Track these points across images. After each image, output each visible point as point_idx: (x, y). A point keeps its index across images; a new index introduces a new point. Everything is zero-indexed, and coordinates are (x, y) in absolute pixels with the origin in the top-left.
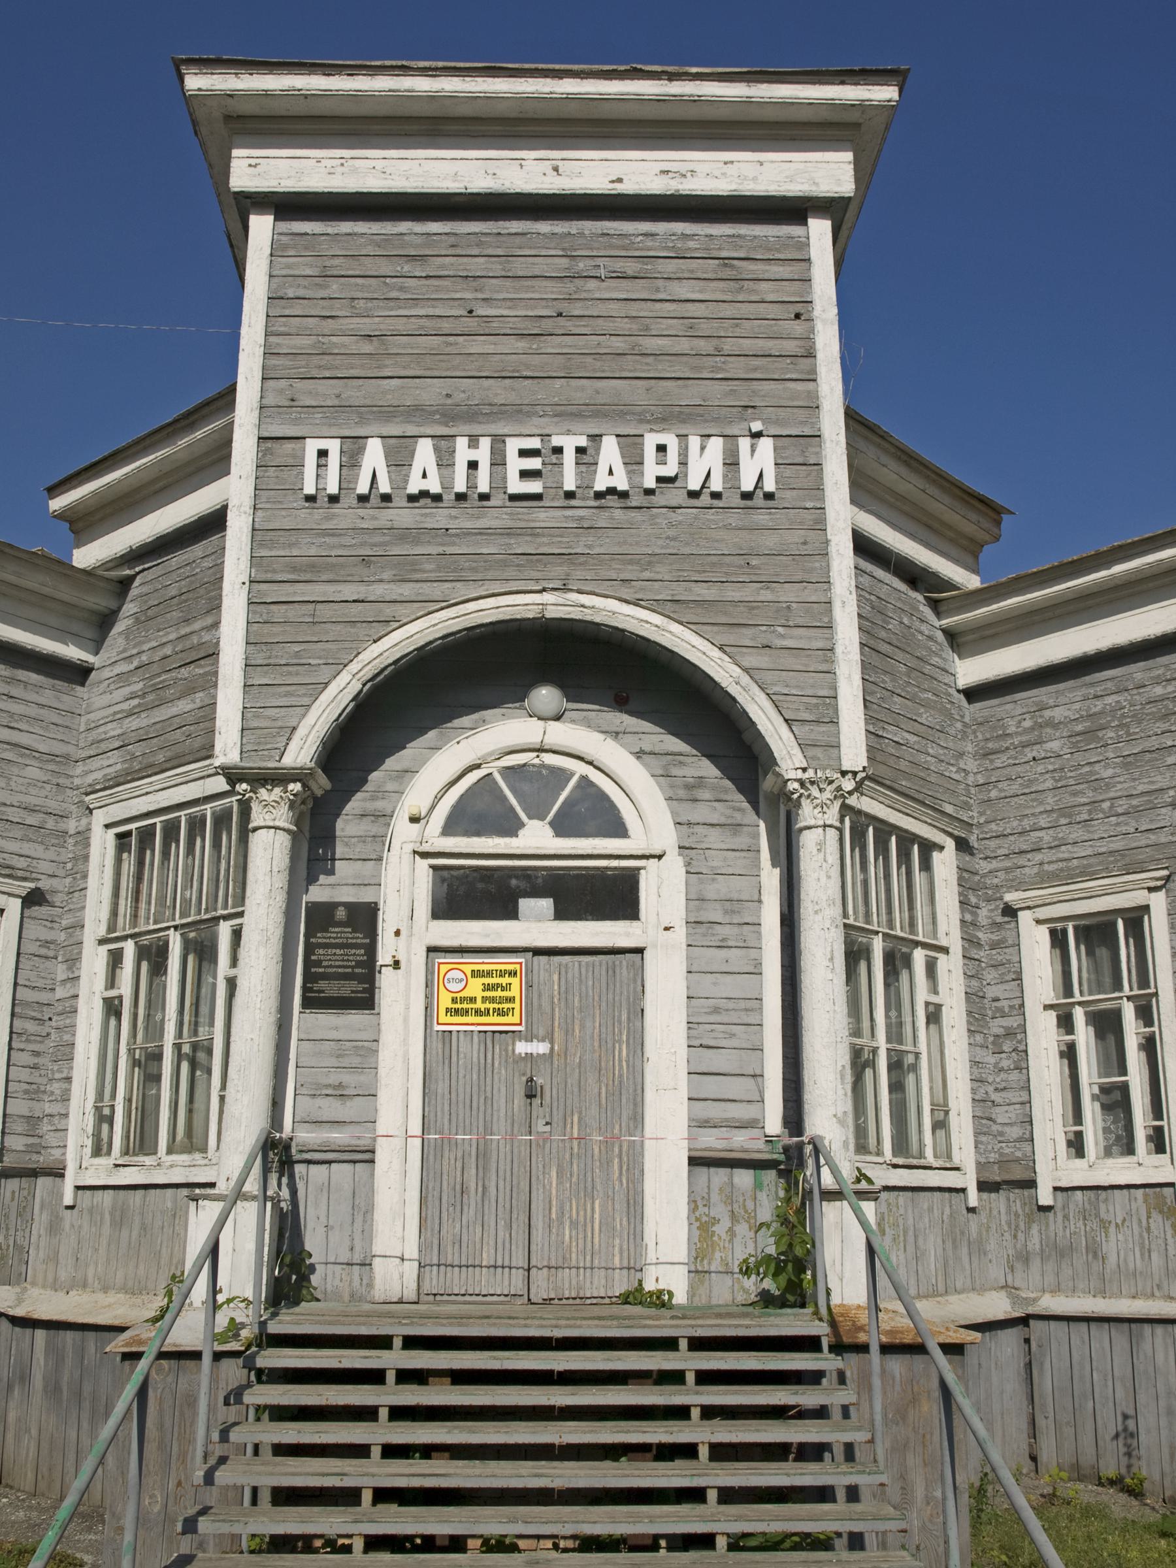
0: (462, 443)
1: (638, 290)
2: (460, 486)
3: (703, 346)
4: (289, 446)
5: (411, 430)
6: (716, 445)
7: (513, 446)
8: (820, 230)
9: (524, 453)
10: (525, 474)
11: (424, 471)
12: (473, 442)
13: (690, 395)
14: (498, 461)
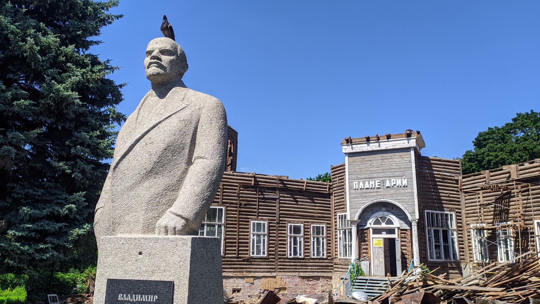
1: (390, 160)
3: (399, 167)
6: (400, 180)
7: (377, 181)
8: (412, 152)
11: (367, 186)
13: (397, 174)
14: (375, 184)
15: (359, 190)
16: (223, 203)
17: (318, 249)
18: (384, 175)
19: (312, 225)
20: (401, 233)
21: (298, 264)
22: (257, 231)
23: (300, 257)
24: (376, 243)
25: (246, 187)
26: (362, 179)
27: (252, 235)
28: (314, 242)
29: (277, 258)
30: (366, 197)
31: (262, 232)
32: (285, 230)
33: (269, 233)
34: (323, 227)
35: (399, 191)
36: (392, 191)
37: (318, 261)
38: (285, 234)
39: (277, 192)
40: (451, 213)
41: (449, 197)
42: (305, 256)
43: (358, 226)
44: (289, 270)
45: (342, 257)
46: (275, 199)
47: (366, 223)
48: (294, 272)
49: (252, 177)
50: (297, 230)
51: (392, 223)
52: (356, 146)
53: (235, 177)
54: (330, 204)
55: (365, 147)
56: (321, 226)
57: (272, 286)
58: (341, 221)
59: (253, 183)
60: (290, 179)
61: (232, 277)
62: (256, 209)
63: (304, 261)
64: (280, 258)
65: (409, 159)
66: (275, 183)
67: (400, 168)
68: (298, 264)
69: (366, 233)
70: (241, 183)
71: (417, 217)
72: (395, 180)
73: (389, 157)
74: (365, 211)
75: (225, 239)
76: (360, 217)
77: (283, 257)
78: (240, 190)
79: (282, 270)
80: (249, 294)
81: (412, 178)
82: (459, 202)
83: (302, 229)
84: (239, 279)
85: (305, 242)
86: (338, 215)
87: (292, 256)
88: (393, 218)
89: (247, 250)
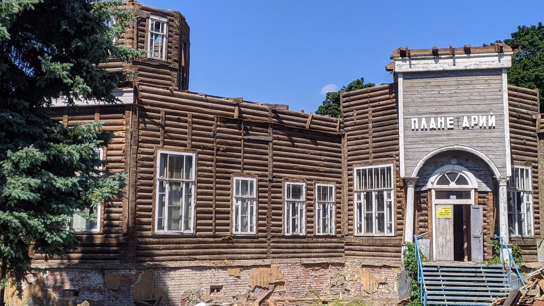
0: (439, 118)
2: (439, 127)
4: (408, 120)
5: (430, 116)
6: (485, 117)
7: (448, 119)
8: (505, 76)
9: (450, 120)
10: (451, 124)
11: (433, 125)
12: (441, 119)
13: (479, 108)
14: (446, 122)
15: (420, 131)
16: (193, 146)
17: (324, 220)
18: (459, 108)
19: (317, 185)
20: (479, 197)
21: (297, 245)
22: (242, 194)
23: (301, 234)
24: (442, 211)
25: (226, 120)
26: (424, 114)
27: (234, 200)
28: (319, 211)
29: (269, 237)
30: (430, 142)
31: (248, 196)
32: (280, 193)
33: (259, 197)
34: (331, 188)
35: (482, 135)
36: (471, 134)
37: (323, 239)
38: (281, 198)
39: (270, 130)
40: (527, 168)
41: (524, 144)
42: (308, 233)
43: (416, 187)
44: (286, 255)
45: (363, 233)
46: (267, 142)
47: (427, 182)
48: (293, 257)
49: (235, 105)
50: (296, 192)
51: (466, 183)
52: (418, 62)
53: (210, 104)
54: (340, 152)
55: (431, 65)
56: (329, 185)
57: (265, 280)
58: (358, 179)
59: (236, 114)
60: (291, 110)
61: (210, 268)
62: (240, 157)
63: (305, 240)
64: (273, 237)
65: (499, 86)
66: (266, 116)
67: (485, 100)
68: (297, 245)
69: (425, 197)
70: (218, 114)
71: (509, 173)
72: (476, 117)
73: (468, 82)
74: (427, 163)
75: (197, 206)
76: (420, 173)
77: (278, 235)
78: (218, 126)
79: (276, 255)
80: (233, 294)
81: (502, 115)
82: (536, 152)
83: (304, 190)
84: (220, 271)
85: (308, 211)
86: (355, 169)
87: (290, 234)
88: (469, 176)
89: (228, 225)
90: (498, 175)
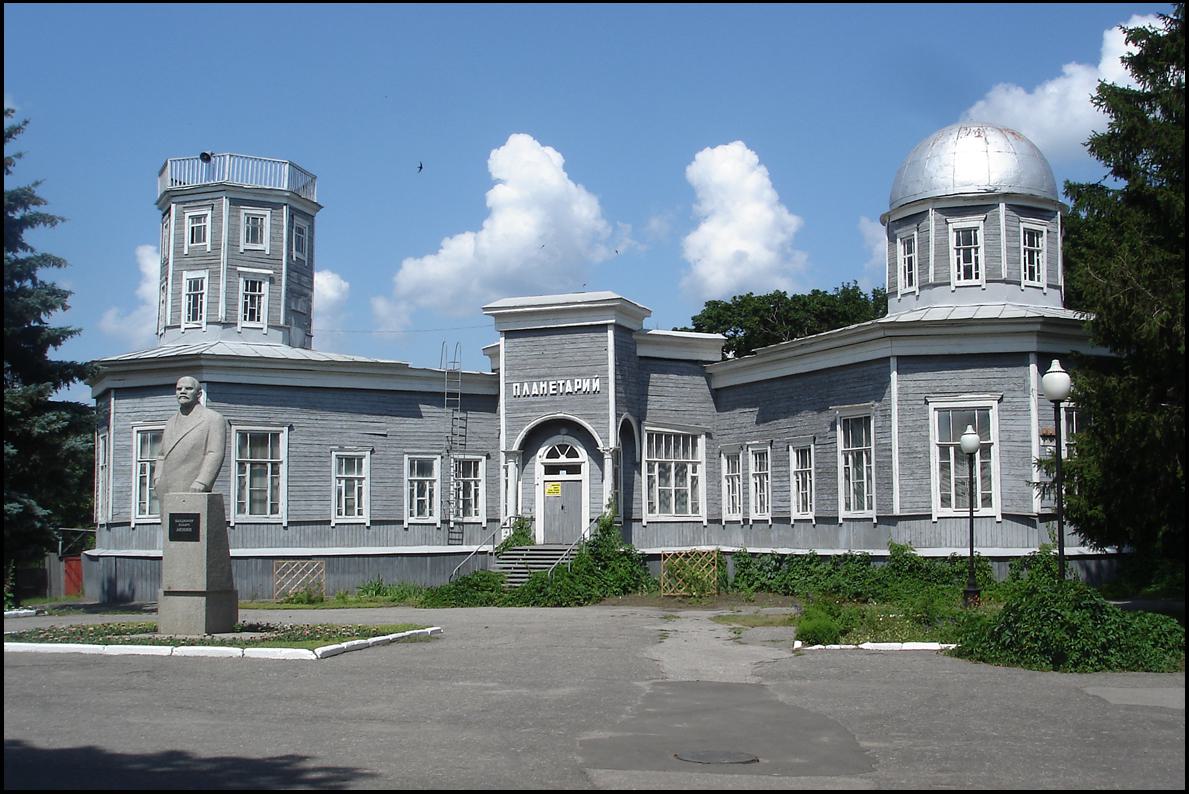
7: (551, 383)
10: (554, 389)
14: (548, 386)
72: (580, 381)
90: (601, 447)
